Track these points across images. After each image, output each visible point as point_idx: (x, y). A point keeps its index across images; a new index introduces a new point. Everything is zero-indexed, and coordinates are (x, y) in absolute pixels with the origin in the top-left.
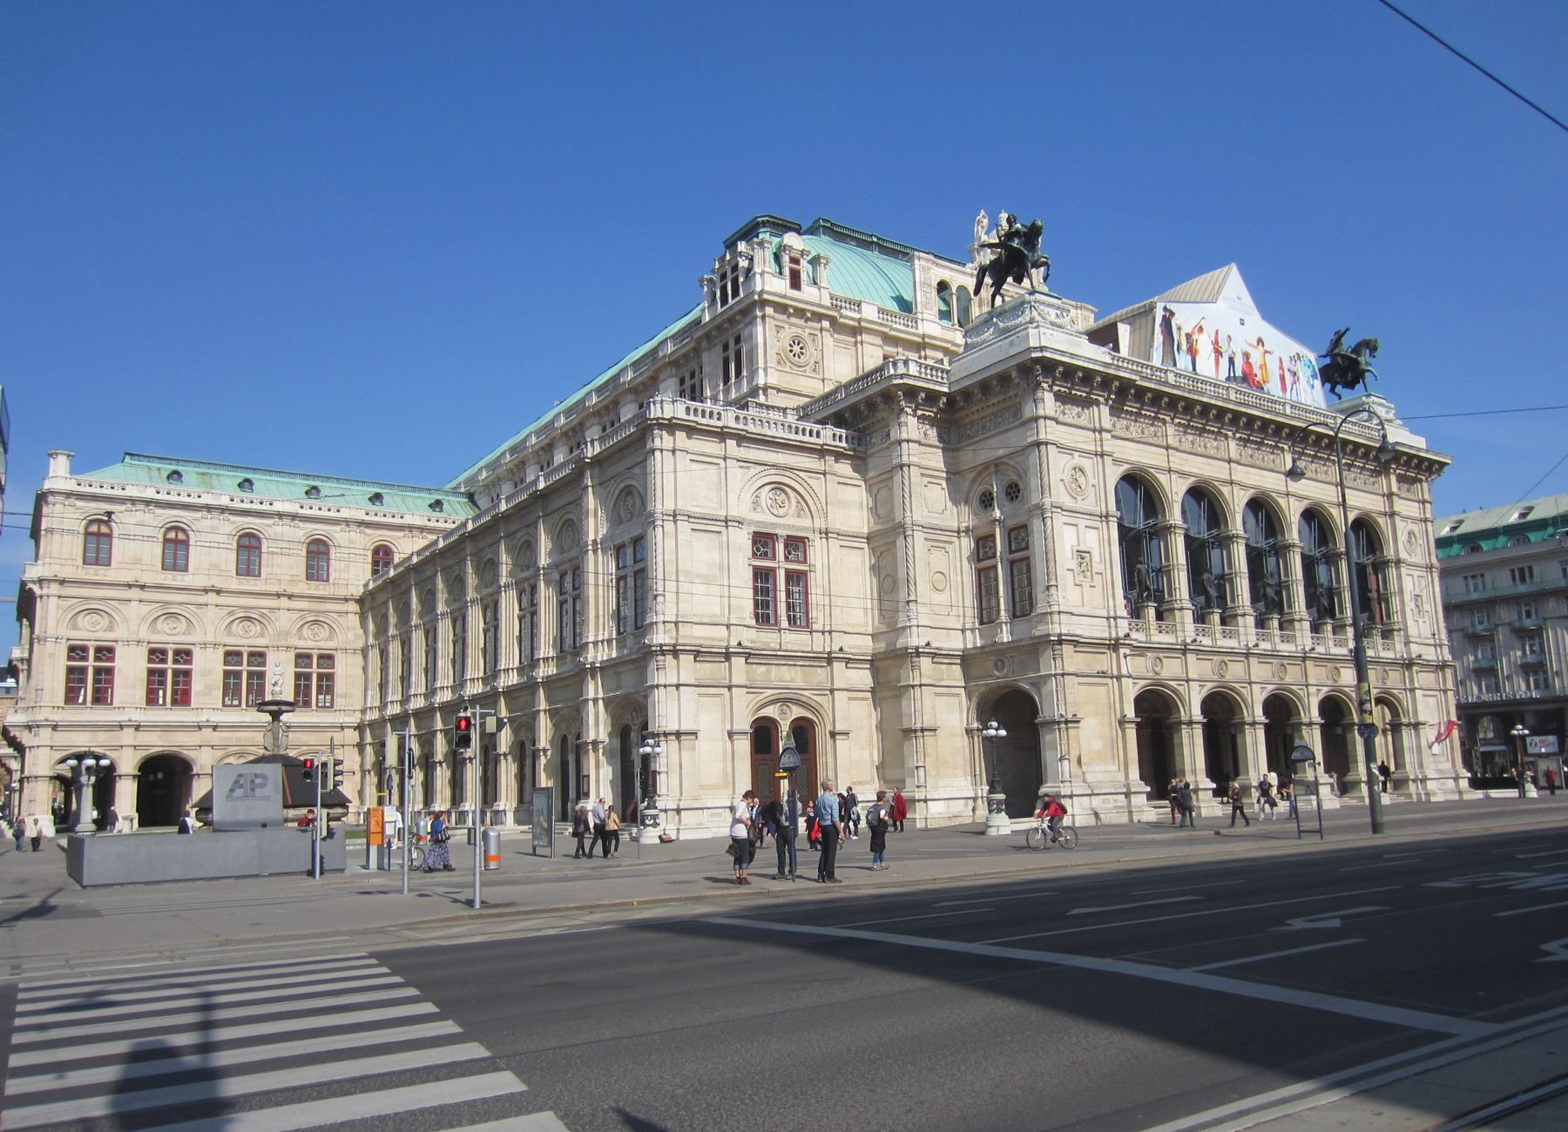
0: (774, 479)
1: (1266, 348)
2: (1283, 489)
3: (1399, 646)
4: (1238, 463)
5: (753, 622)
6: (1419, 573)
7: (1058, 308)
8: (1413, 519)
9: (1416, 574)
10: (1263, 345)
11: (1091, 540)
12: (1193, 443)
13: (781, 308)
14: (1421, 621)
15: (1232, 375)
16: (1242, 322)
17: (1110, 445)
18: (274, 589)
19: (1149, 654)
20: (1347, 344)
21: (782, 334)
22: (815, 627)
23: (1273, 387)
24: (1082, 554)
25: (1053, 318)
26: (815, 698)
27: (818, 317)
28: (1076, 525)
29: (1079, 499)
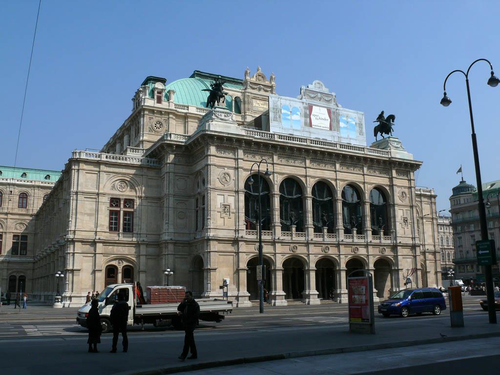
0: (121, 178)
4: (310, 168)
5: (108, 230)
6: (406, 209)
8: (405, 187)
9: (405, 209)
11: (231, 200)
13: (152, 111)
14: (406, 228)
18: (6, 211)
20: (386, 116)
21: (152, 120)
22: (134, 232)
24: (226, 207)
25: (223, 117)
26: (132, 258)
27: (168, 113)
28: (224, 195)
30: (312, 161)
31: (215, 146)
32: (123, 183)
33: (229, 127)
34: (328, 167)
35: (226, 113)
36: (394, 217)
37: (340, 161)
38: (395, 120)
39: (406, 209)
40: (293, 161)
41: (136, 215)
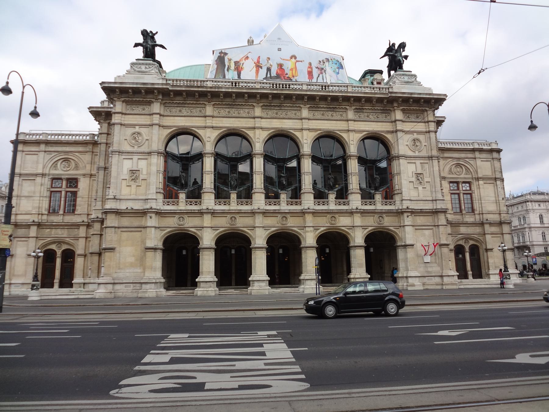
1: (297, 60)
2: (299, 127)
3: (398, 202)
4: (261, 118)
5: (46, 213)
6: (422, 161)
7: (146, 64)
9: (418, 162)
10: (295, 58)
12: (229, 112)
14: (420, 188)
15: (269, 76)
16: (279, 50)
17: (156, 119)
19: (177, 216)
23: (303, 78)
28: (132, 159)
29: (136, 147)
30: (264, 107)
31: (123, 102)
32: (66, 162)
33: (143, 78)
34: (291, 114)
35: (146, 64)
36: (399, 174)
37: (308, 106)
38: (406, 48)
39: (422, 161)
40: (236, 112)
41: (79, 194)
